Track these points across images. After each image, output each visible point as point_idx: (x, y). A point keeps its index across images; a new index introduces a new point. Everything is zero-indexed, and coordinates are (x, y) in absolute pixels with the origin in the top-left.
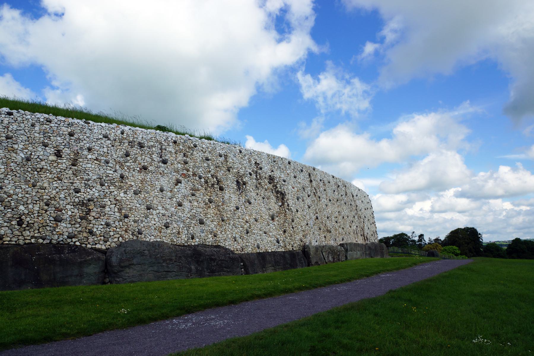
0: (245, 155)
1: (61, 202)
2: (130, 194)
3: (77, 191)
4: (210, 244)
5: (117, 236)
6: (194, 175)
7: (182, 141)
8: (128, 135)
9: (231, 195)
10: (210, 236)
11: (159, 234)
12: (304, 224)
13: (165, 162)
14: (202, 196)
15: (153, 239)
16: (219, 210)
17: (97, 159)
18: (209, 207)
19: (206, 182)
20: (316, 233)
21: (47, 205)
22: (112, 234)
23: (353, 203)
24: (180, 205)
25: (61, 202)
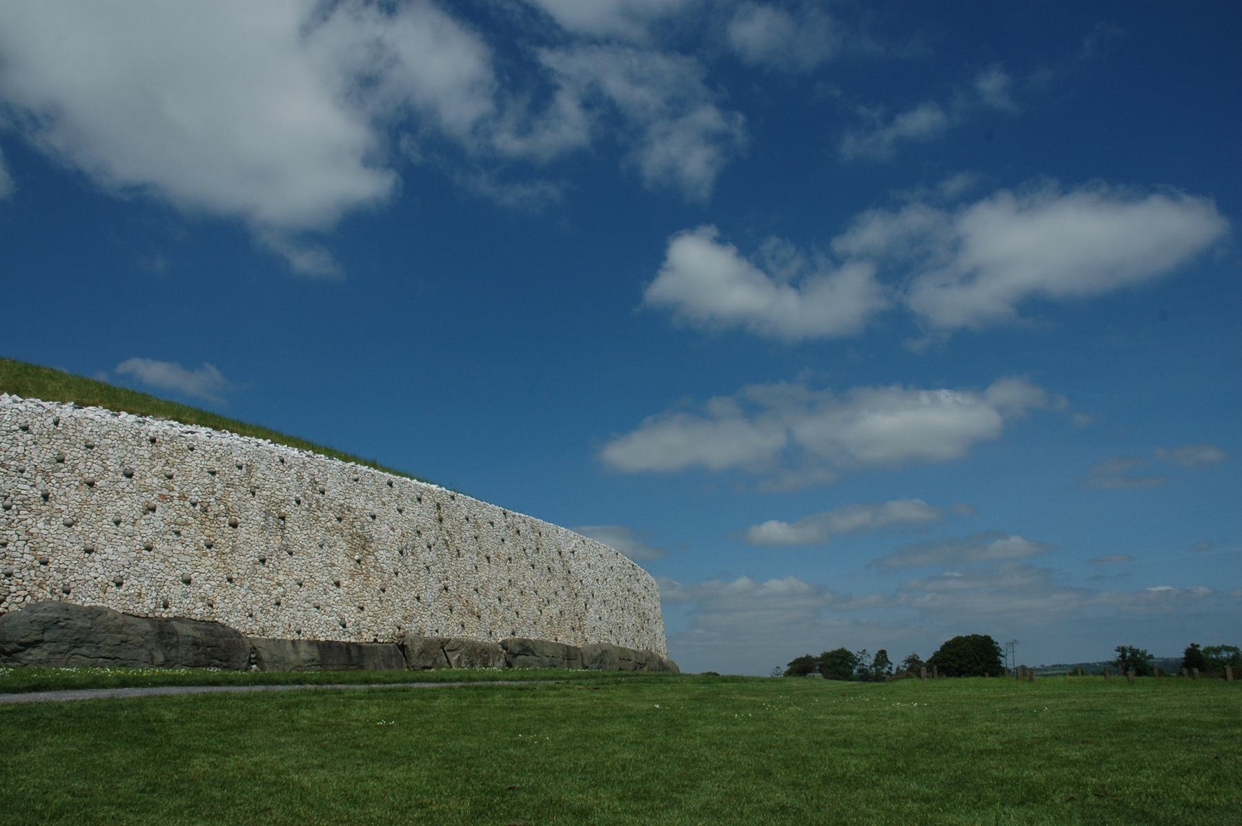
0: (291, 467)
2: (57, 524)
4: (199, 617)
5: (23, 593)
6: (183, 497)
7: (167, 438)
9: (252, 539)
10: (200, 604)
11: (102, 594)
12: (409, 596)
13: (129, 475)
14: (194, 534)
15: (89, 603)
18: (205, 555)
20: (439, 614)
22: (13, 589)
23: (557, 566)
24: (149, 549)
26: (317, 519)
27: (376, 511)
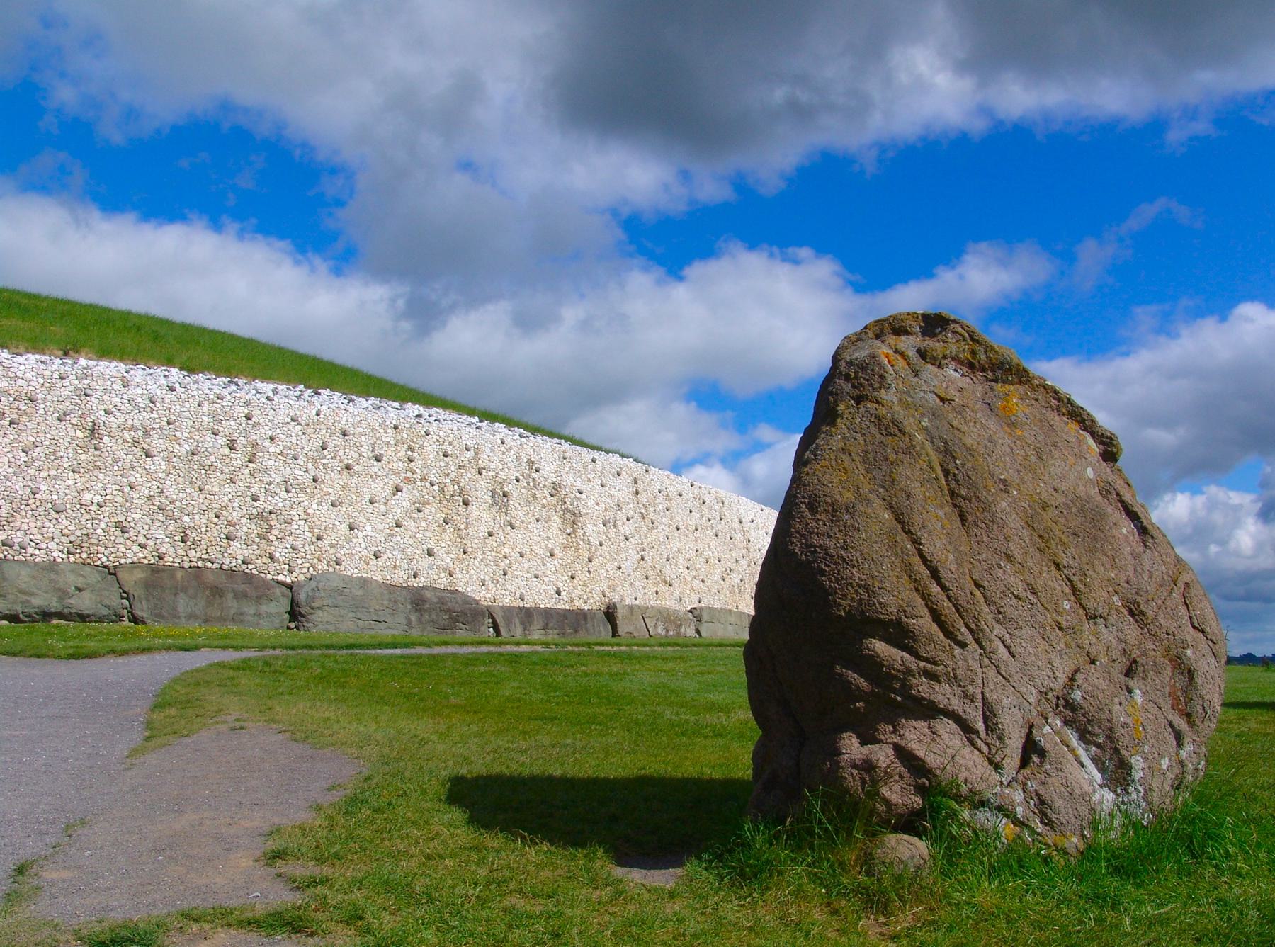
0: (510, 449)
1: (235, 514)
3: (255, 499)
6: (423, 479)
8: (326, 417)
9: (482, 515)
10: (443, 575)
12: (611, 567)
13: (378, 459)
15: (356, 573)
16: (459, 536)
17: (281, 454)
18: (444, 530)
19: (442, 491)
20: (637, 583)
21: (217, 517)
23: (738, 536)
25: (235, 514)
26: (534, 496)
27: (583, 488)
